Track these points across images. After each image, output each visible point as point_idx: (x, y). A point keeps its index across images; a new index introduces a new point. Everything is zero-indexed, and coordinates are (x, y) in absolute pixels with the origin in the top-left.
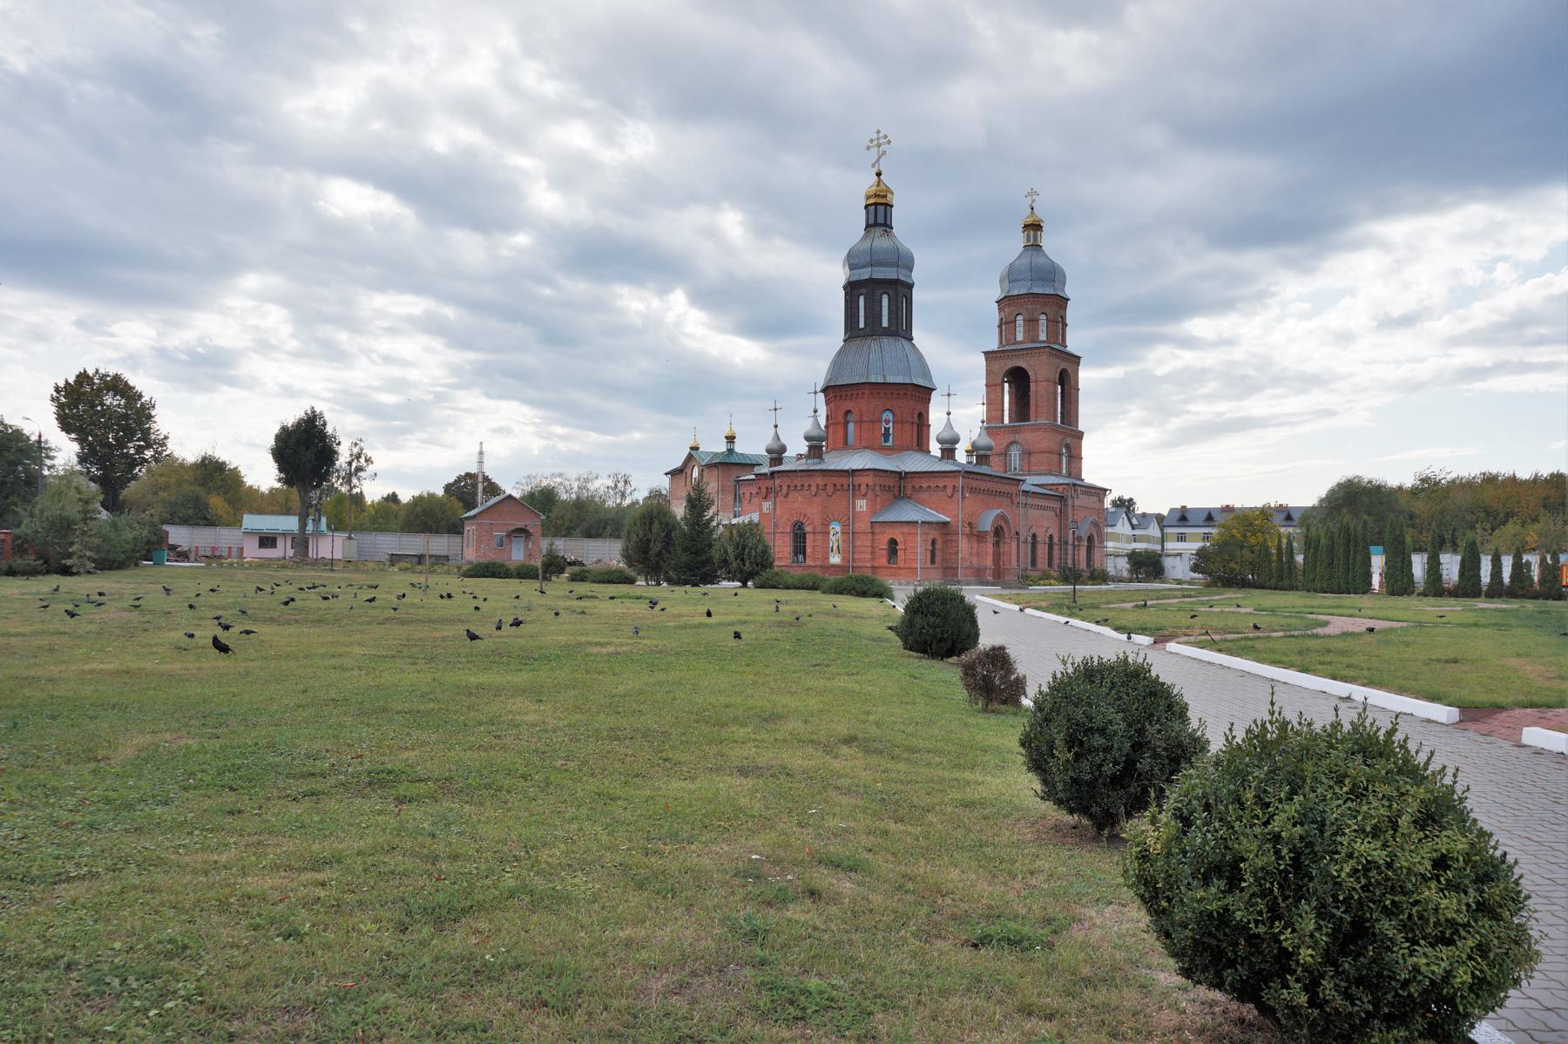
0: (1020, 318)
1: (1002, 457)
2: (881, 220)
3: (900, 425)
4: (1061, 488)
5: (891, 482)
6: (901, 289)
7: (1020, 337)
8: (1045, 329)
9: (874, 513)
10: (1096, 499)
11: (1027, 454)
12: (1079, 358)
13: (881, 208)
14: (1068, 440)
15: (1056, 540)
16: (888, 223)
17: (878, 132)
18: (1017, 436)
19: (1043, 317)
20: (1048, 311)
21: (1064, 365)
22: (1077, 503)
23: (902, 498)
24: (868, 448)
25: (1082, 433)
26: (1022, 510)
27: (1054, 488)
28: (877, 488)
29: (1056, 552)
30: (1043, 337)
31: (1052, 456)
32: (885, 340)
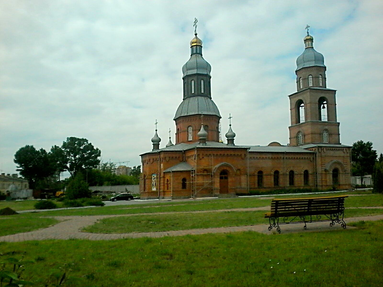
0: (301, 79)
1: (296, 138)
2: (195, 52)
3: (194, 132)
4: (314, 149)
5: (177, 155)
6: (199, 77)
7: (301, 87)
8: (312, 81)
9: (164, 169)
10: (341, 152)
11: (304, 135)
12: (335, 91)
13: (198, 47)
14: (327, 127)
15: (310, 172)
16: (198, 52)
17: (195, 18)
18: (300, 129)
19: (311, 76)
20: (312, 73)
21: (322, 95)
22: (323, 155)
23: (184, 162)
24: (182, 142)
25: (339, 123)
26: (282, 161)
27: (311, 149)
28: (167, 159)
29: (310, 178)
30: (311, 85)
31: (314, 135)
32: (192, 98)
